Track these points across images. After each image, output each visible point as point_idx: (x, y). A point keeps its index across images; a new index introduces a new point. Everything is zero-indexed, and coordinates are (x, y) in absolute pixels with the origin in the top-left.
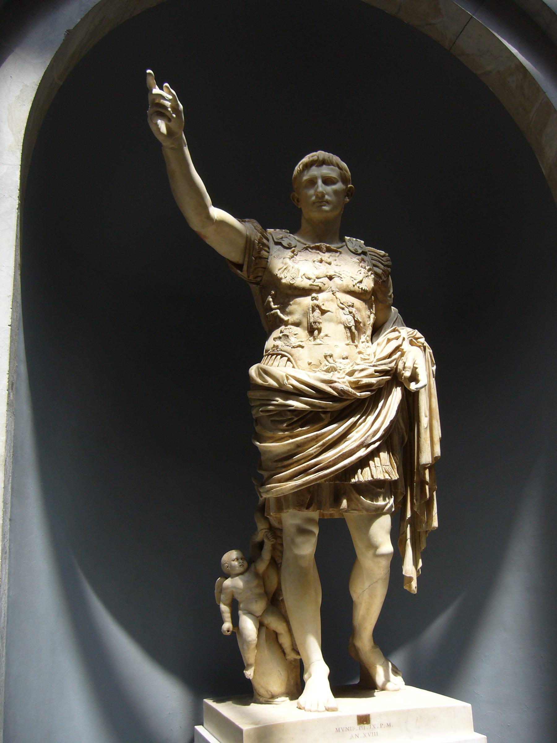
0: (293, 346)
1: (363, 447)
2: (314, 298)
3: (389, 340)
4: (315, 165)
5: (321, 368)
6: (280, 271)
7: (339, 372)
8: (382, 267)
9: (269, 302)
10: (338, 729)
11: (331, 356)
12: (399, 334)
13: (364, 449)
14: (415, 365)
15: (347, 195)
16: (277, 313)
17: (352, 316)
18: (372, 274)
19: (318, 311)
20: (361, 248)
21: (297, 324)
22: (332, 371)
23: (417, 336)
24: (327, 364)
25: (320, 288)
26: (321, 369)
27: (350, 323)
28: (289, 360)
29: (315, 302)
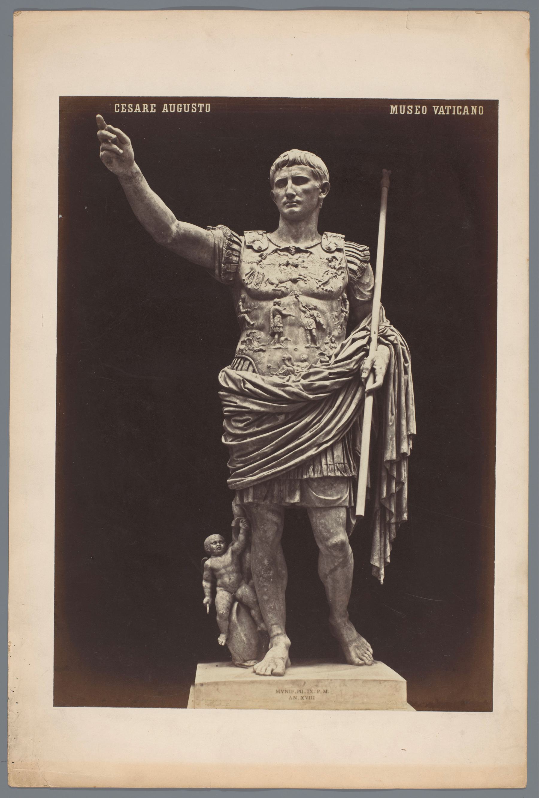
0: (255, 351)
1: (315, 447)
2: (275, 303)
3: (354, 340)
4: (286, 166)
5: (279, 371)
6: (247, 276)
7: (296, 375)
8: (358, 262)
9: (239, 306)
10: (278, 691)
11: (289, 359)
12: (369, 333)
13: (316, 448)
14: (374, 366)
15: (323, 192)
16: (244, 317)
17: (313, 319)
18: (342, 272)
19: (278, 316)
20: (335, 245)
21: (261, 328)
22: (289, 374)
23: (387, 334)
24: (286, 367)
25: (283, 292)
26: (279, 372)
27: (310, 326)
28: (251, 363)
29: (277, 307)
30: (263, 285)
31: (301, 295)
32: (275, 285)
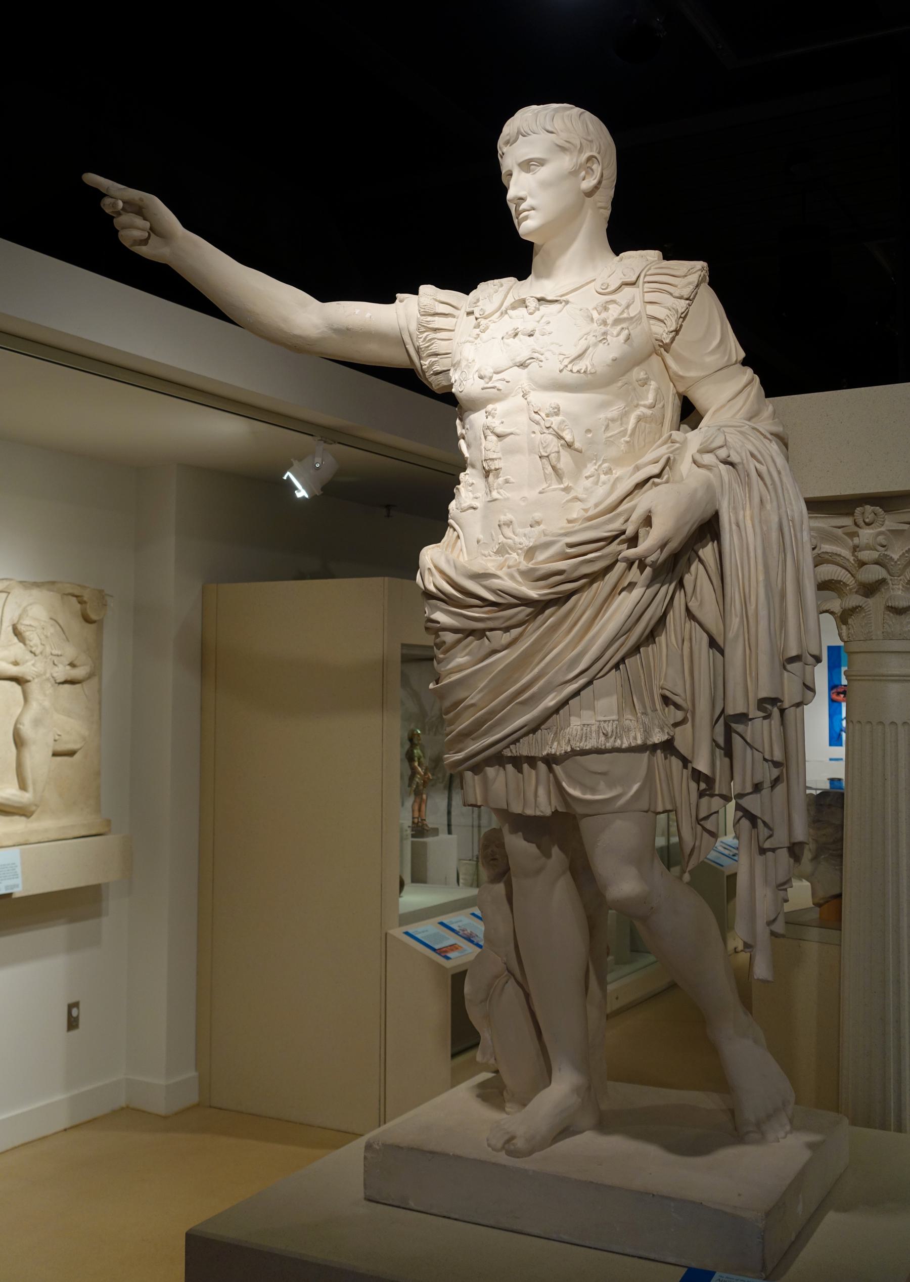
30: (471, 381)
31: (533, 390)
32: (487, 380)
